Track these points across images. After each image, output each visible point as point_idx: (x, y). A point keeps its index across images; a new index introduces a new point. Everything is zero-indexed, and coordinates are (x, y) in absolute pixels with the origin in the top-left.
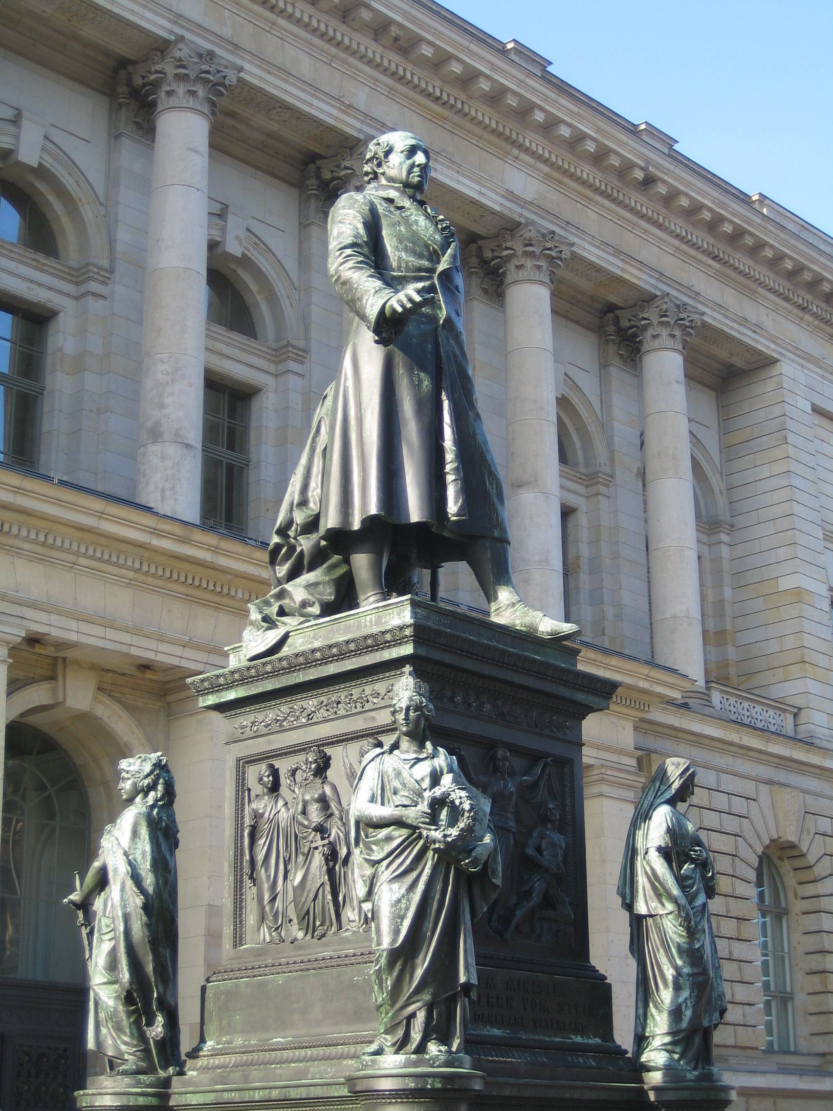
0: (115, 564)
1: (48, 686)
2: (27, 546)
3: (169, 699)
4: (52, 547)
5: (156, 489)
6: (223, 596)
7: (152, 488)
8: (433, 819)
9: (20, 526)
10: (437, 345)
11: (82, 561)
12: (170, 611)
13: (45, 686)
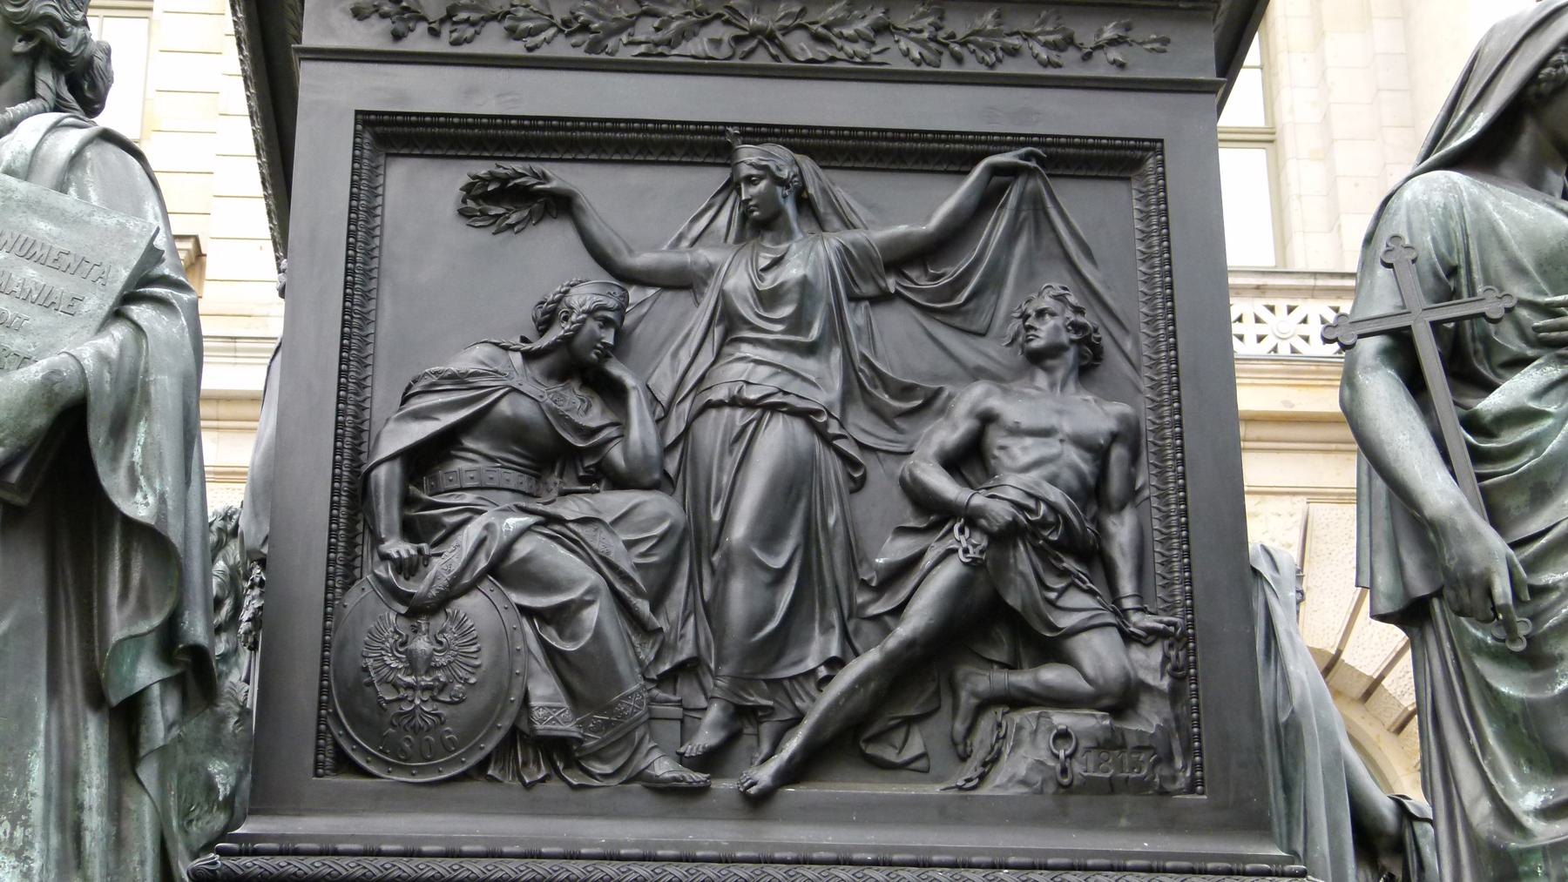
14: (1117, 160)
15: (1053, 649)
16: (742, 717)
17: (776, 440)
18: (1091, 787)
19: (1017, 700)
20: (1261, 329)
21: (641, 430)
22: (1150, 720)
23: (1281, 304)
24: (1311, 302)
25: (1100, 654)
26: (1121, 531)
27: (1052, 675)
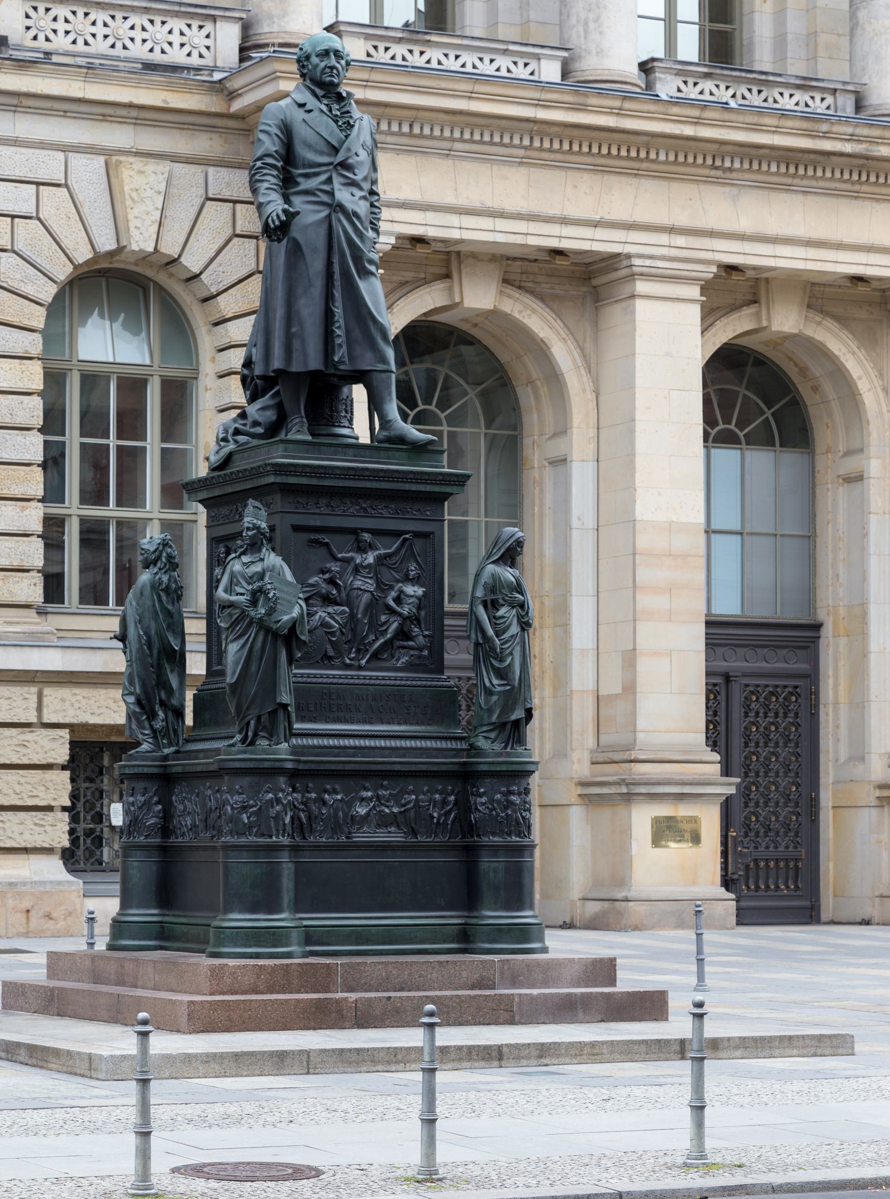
0: (501, 144)
1: (442, 285)
2: (389, 139)
3: (595, 282)
4: (421, 136)
5: (578, 21)
6: (642, 160)
7: (573, 20)
8: (254, 603)
9: (380, 119)
11: (458, 146)
12: (575, 187)
13: (439, 286)
14: (425, 535)
15: (409, 638)
16: (358, 651)
17: (366, 597)
18: (416, 665)
19: (404, 647)
20: (145, 35)
21: (344, 595)
22: (426, 653)
23: (158, 19)
24: (175, 20)
26: (423, 613)
27: (411, 643)
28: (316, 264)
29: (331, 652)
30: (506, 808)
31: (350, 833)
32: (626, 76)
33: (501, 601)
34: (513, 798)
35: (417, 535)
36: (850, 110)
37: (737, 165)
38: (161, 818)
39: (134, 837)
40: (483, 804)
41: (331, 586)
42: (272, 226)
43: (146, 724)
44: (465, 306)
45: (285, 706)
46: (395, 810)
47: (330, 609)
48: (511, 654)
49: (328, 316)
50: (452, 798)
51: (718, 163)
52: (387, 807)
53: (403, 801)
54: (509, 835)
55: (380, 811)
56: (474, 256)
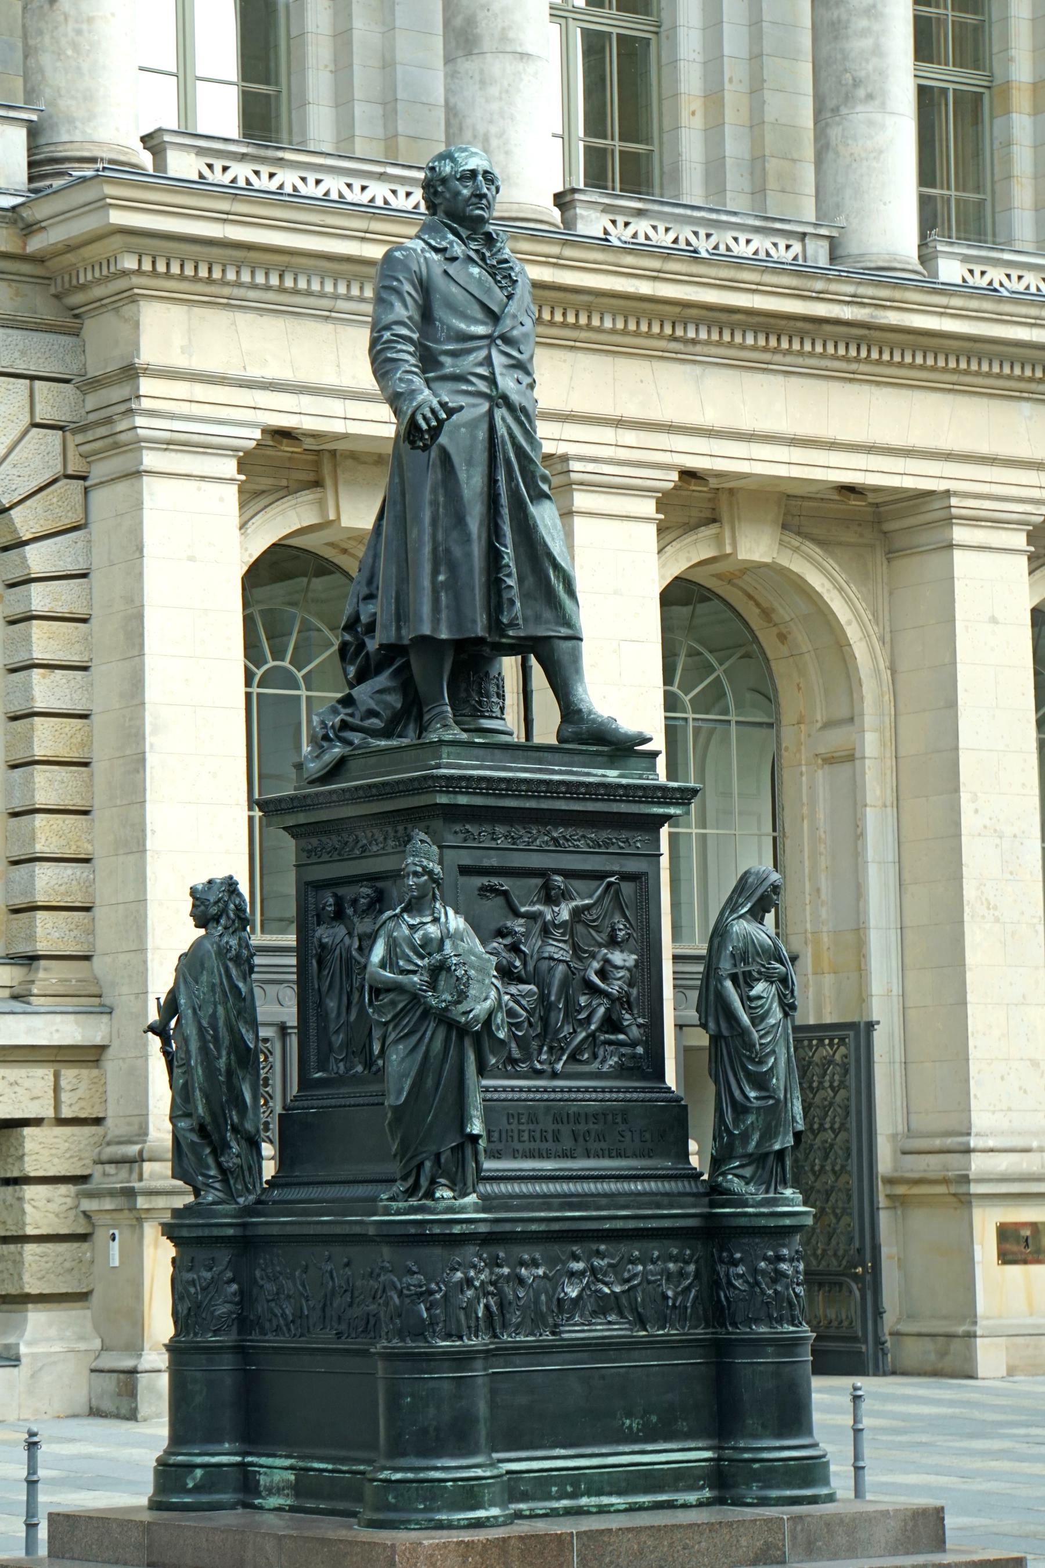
1: (311, 497)
8: (433, 985)
9: (239, 267)
10: (492, 429)
11: (341, 305)
15: (621, 1030)
16: (551, 1049)
25: (635, 1032)
28: (472, 483)
29: (516, 1053)
30: (774, 1281)
31: (556, 1326)
32: (541, 212)
33: (755, 974)
34: (784, 1266)
35: (625, 877)
36: (823, 261)
37: (703, 335)
38: (237, 1304)
39: (196, 1334)
40: (739, 1276)
41: (513, 955)
42: (425, 426)
43: (210, 1161)
44: (343, 525)
45: (475, 1139)
46: (617, 1289)
47: (513, 990)
48: (773, 1052)
49: (494, 556)
50: (692, 1268)
51: (679, 332)
52: (606, 1284)
53: (626, 1275)
54: (780, 1321)
55: (596, 1291)
56: (354, 456)
